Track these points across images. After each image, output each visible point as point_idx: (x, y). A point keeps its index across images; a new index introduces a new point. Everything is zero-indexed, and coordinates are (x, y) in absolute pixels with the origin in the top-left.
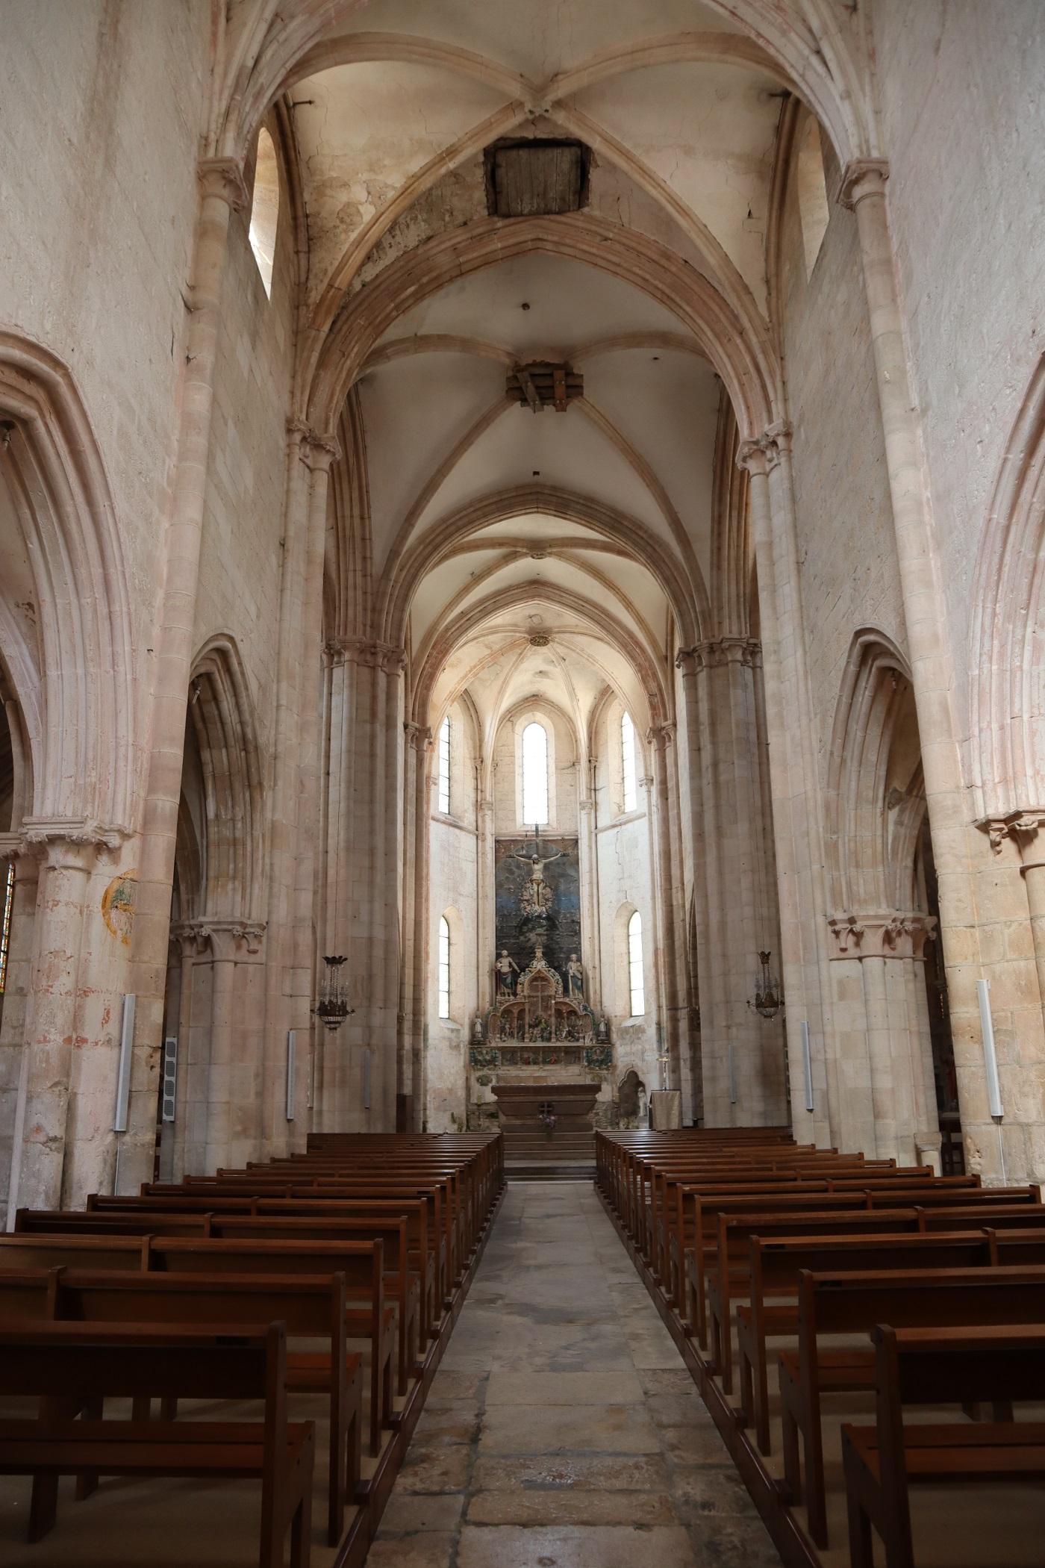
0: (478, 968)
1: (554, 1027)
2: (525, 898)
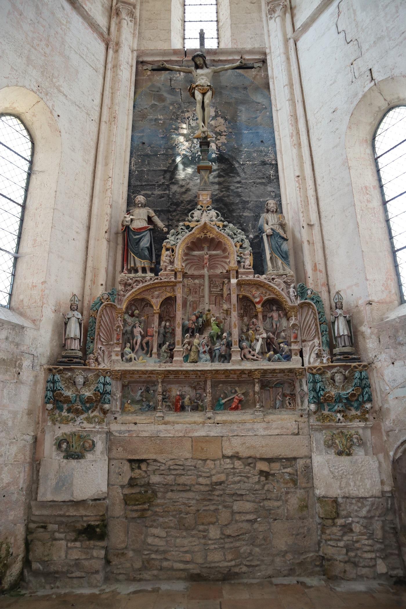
0: (89, 228)
1: (236, 332)
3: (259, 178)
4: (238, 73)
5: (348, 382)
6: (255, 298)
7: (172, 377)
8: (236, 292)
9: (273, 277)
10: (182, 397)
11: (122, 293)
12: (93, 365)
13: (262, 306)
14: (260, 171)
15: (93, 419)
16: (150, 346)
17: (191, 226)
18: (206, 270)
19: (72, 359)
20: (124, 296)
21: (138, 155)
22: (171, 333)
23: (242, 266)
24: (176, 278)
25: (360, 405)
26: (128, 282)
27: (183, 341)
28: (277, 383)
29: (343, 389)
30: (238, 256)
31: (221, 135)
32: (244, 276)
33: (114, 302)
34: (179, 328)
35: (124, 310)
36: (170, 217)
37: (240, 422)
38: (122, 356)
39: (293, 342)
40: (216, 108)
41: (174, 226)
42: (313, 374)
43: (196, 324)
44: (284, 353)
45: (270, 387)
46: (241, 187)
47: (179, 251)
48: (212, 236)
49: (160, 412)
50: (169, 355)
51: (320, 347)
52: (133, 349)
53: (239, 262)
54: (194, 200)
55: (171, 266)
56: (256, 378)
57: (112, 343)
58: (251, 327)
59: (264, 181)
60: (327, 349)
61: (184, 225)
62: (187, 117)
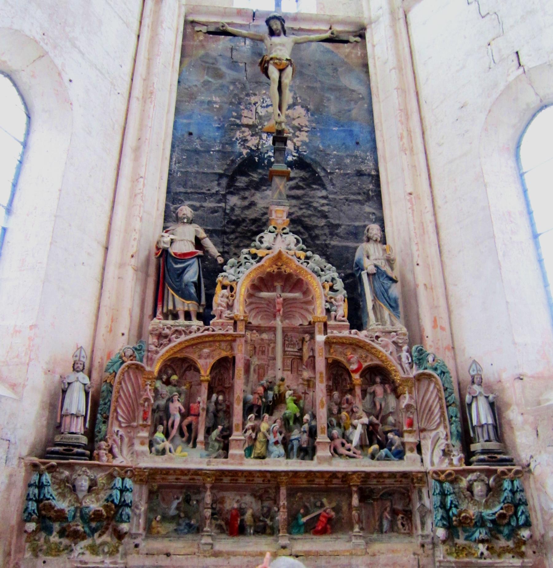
1: (322, 413)
2: (245, 121)
3: (354, 194)
4: (326, 48)
5: (493, 495)
6: (351, 364)
7: (226, 480)
8: (324, 353)
9: (377, 334)
10: (241, 511)
11: (153, 348)
12: (105, 458)
13: (361, 376)
14: (355, 184)
15: (101, 549)
16: (194, 430)
17: (260, 255)
18: (278, 319)
19: (71, 448)
20: (157, 352)
21: (182, 150)
22: (225, 412)
23: (333, 316)
24: (235, 329)
25: (513, 533)
26: (164, 332)
27: (244, 424)
28: (384, 494)
29: (487, 505)
30: (327, 302)
31: (300, 130)
32: (335, 332)
33: (141, 361)
34: (238, 404)
35: (156, 374)
36: (226, 241)
37: (330, 553)
38: (151, 445)
39: (406, 431)
40: (295, 94)
41: (231, 254)
42: (441, 482)
43: (264, 400)
44: (393, 448)
45: (374, 500)
46: (327, 205)
47: (242, 290)
48: (288, 270)
49: (208, 535)
50: (222, 445)
51: (447, 440)
52: (167, 434)
53: (328, 311)
54: (260, 219)
55: (229, 312)
56: (354, 485)
57: (135, 424)
58: (344, 406)
59: (360, 198)
60: (458, 444)
61: (249, 253)
62: (253, 102)
